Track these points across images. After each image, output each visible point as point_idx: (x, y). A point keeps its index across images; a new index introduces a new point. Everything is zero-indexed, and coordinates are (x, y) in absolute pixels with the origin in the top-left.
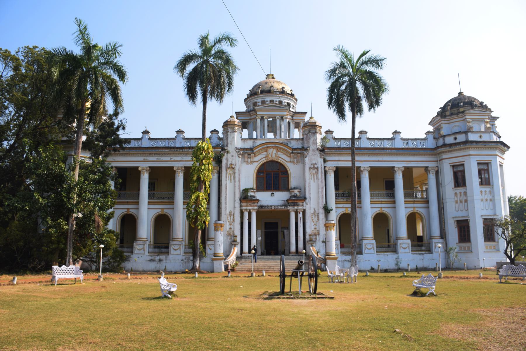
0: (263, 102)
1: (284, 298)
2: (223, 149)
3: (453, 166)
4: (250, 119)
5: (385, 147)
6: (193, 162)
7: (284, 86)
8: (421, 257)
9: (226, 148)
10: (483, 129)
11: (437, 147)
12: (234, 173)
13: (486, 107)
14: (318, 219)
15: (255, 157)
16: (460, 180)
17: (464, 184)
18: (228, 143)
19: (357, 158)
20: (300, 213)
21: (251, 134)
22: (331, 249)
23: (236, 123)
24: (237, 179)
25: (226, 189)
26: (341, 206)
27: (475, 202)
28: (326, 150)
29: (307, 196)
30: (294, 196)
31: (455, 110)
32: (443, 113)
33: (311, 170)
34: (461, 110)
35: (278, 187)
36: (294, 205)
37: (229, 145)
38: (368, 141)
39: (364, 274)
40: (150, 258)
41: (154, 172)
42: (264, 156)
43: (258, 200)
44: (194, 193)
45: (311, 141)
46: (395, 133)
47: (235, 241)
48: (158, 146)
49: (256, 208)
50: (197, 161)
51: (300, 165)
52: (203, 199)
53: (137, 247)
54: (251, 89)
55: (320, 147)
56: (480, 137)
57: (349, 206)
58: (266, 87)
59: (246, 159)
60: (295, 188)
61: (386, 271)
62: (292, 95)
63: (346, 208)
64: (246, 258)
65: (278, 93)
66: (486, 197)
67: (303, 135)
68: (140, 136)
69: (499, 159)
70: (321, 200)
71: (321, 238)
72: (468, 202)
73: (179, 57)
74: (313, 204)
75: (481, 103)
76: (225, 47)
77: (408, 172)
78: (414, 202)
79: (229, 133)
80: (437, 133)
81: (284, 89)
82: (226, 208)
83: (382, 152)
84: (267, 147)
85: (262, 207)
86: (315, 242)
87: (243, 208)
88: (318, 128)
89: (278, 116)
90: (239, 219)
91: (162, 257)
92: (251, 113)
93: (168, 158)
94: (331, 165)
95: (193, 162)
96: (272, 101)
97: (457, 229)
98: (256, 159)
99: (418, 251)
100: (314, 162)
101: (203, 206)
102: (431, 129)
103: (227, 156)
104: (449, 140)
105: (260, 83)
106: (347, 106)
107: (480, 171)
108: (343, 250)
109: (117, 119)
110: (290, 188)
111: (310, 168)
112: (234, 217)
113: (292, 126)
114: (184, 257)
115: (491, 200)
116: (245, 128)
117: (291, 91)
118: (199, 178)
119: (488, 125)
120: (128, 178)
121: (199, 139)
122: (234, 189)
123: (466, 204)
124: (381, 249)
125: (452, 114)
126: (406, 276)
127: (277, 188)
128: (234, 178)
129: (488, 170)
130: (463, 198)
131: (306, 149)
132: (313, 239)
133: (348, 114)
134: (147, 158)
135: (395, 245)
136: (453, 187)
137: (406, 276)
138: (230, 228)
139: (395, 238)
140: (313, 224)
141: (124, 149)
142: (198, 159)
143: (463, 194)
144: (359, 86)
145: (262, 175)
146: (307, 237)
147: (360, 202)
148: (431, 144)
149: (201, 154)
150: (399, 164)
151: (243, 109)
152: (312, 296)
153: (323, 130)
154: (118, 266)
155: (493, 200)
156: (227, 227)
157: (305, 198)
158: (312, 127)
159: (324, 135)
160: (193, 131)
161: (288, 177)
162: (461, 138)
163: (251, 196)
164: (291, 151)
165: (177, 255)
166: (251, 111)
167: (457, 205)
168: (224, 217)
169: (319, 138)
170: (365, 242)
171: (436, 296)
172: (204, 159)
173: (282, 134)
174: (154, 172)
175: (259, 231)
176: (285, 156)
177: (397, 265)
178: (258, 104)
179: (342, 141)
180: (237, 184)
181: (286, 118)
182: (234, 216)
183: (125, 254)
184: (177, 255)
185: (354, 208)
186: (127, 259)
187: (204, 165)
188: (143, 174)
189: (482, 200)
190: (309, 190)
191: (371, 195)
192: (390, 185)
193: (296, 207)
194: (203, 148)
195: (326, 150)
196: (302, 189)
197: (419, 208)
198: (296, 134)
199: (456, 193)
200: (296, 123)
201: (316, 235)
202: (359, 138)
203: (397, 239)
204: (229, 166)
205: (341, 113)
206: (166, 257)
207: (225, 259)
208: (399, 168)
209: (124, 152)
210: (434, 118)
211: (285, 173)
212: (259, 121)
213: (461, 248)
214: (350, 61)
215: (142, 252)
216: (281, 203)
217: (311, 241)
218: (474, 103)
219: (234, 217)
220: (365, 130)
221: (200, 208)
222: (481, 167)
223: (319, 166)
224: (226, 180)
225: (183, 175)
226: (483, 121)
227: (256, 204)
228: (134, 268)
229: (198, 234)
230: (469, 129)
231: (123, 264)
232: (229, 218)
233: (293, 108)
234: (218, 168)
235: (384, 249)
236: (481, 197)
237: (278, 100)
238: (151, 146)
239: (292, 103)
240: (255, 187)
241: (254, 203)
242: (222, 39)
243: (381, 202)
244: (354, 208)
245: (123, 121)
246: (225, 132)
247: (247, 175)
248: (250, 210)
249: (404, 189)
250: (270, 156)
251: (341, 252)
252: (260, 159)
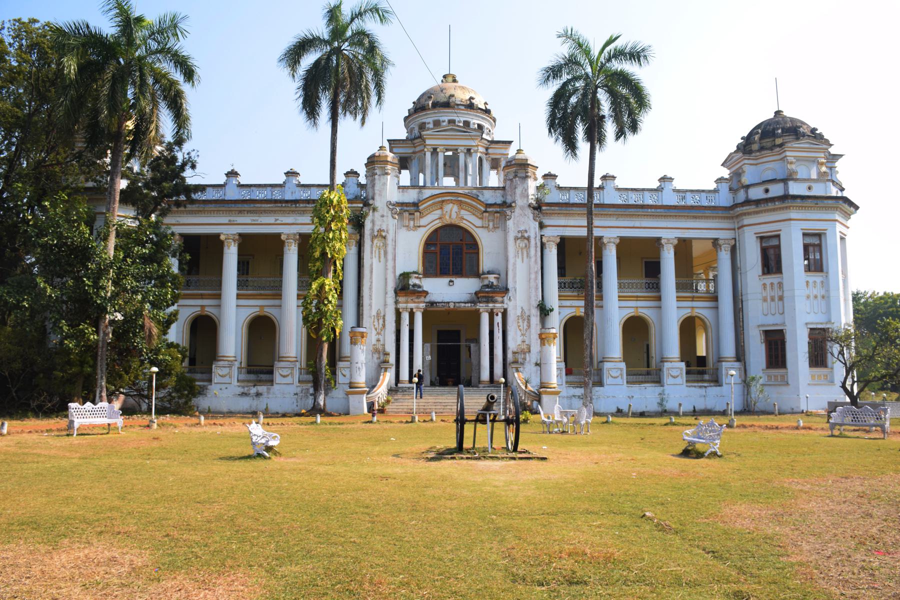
0: (437, 123)
1: (462, 458)
2: (366, 204)
3: (762, 238)
4: (414, 153)
5: (646, 203)
6: (313, 227)
7: (473, 96)
8: (702, 391)
9: (371, 202)
10: (814, 176)
11: (736, 206)
12: (385, 245)
13: (821, 136)
14: (529, 326)
15: (421, 217)
16: (772, 262)
17: (779, 270)
18: (374, 194)
19: (596, 222)
20: (497, 315)
21: (414, 179)
22: (550, 377)
23: (389, 159)
24: (390, 257)
25: (371, 272)
26: (568, 303)
27: (796, 298)
28: (544, 208)
29: (510, 286)
30: (487, 286)
31: (767, 142)
32: (747, 147)
33: (518, 241)
34: (779, 141)
35: (461, 270)
36: (488, 302)
37: (377, 197)
38: (617, 193)
39: (604, 419)
40: (242, 390)
41: (247, 243)
42: (437, 217)
43: (426, 293)
44: (316, 279)
45: (518, 191)
46: (664, 179)
47: (386, 362)
48: (253, 198)
49: (422, 305)
50: (321, 225)
51: (499, 233)
52: (331, 290)
53: (218, 371)
54: (415, 100)
55: (534, 203)
56: (809, 188)
57: (582, 303)
58: (442, 98)
59: (406, 222)
60: (489, 273)
61: (642, 415)
62: (487, 111)
63: (576, 307)
64: (404, 390)
65: (463, 108)
66: (815, 292)
67: (505, 180)
68: (222, 180)
69: (839, 228)
70: (533, 293)
71: (533, 357)
72: (785, 299)
73: (289, 40)
74: (520, 300)
75: (814, 130)
76: (370, 25)
77: (683, 248)
78: (693, 299)
79: (376, 177)
80: (734, 179)
81: (473, 101)
82: (371, 305)
83: (640, 211)
84: (443, 201)
85: (432, 303)
86: (522, 364)
87: (401, 306)
88: (530, 169)
89: (462, 148)
90: (394, 324)
91: (262, 389)
92: (416, 141)
93: (270, 219)
94: (553, 234)
95: (313, 227)
96: (451, 122)
97: (764, 345)
98: (423, 221)
99: (698, 381)
100: (522, 228)
101: (330, 302)
102: (725, 173)
103: (373, 215)
104: (756, 193)
105: (431, 89)
106: (580, 131)
107: (806, 247)
108: (571, 378)
109: (181, 150)
110: (481, 272)
111: (516, 239)
112: (384, 322)
113: (486, 165)
114: (299, 389)
115: (823, 297)
116: (406, 168)
117: (486, 103)
118: (324, 254)
119: (824, 169)
120: (202, 253)
121: (326, 186)
122: (386, 274)
123: (780, 303)
124: (634, 378)
125: (762, 149)
126: (674, 424)
127: (459, 272)
128: (386, 253)
129: (819, 246)
130: (776, 293)
131: (510, 206)
132: (520, 360)
133: (583, 147)
134: (235, 219)
135: (659, 371)
136: (760, 273)
137: (674, 424)
138: (378, 340)
139: (658, 360)
140: (519, 333)
141: (193, 202)
142: (322, 220)
143: (776, 286)
144: (603, 96)
145: (433, 248)
146: (510, 356)
147: (601, 298)
148: (724, 199)
149: (328, 212)
150: (668, 232)
151: (402, 134)
152: (510, 455)
153: (540, 173)
154: (186, 403)
155: (826, 297)
156: (372, 337)
157: (506, 290)
158: (519, 168)
159: (540, 181)
160: (314, 172)
161: (478, 253)
162: (776, 190)
163: (414, 285)
164: (483, 209)
165: (287, 385)
166: (416, 138)
167: (765, 304)
168: (366, 320)
169: (532, 186)
170: (607, 365)
171: (720, 456)
172: (332, 221)
173: (469, 178)
174: (247, 243)
175: (428, 345)
176: (474, 217)
177: (661, 404)
178: (427, 126)
179: (572, 192)
180: (390, 264)
181: (476, 152)
182: (384, 319)
183: (197, 383)
184: (287, 385)
185: (589, 307)
186: (202, 392)
187: (333, 231)
188: (229, 247)
189: (808, 297)
190: (515, 276)
191: (620, 286)
192: (653, 270)
193: (491, 305)
194: (331, 201)
195: (544, 208)
196: (502, 274)
197: (701, 309)
198: (494, 179)
199: (764, 285)
200: (493, 159)
201: (525, 353)
202: (601, 188)
203: (662, 362)
204: (376, 234)
205: (571, 145)
206: (269, 389)
207: (368, 393)
208: (668, 240)
209: (194, 207)
210: (731, 154)
211: (474, 246)
212: (428, 155)
213: (769, 377)
214: (587, 52)
215: (226, 380)
216: (465, 297)
217: (516, 362)
218: (801, 130)
219: (384, 322)
220: (611, 174)
221: (326, 305)
222: (809, 240)
223: (532, 235)
224: (372, 258)
225: (296, 248)
226: (814, 161)
227: (422, 299)
228: (213, 408)
229: (322, 350)
230: (791, 175)
231: (194, 401)
232: (376, 323)
233: (488, 134)
234: (358, 237)
235: (641, 378)
236: (807, 292)
237: (462, 119)
238: (241, 198)
239: (486, 125)
240: (421, 270)
241: (418, 297)
242: (365, 12)
243: (637, 298)
244: (589, 307)
245: (193, 154)
246: (371, 174)
247: (407, 248)
248: (412, 309)
249: (677, 276)
250: (447, 217)
251: (567, 382)
252: (431, 221)
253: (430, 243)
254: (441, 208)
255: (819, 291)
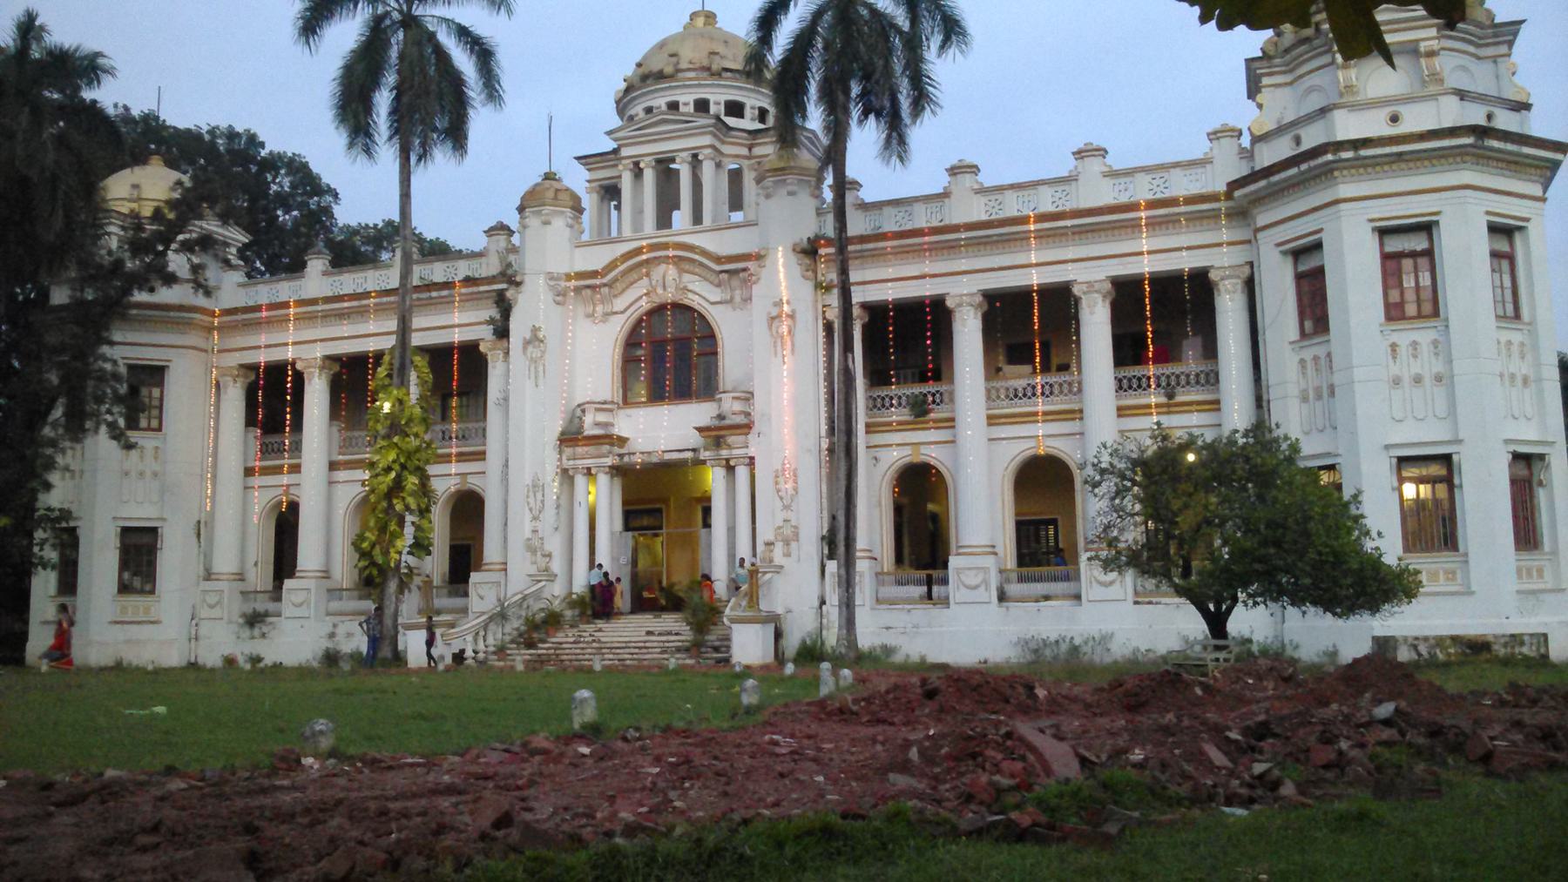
27: (1357, 387)
89: (684, 154)
98: (619, 304)
107: (1391, 262)
115: (1439, 379)
138: (535, 531)
146: (760, 548)
176: (705, 283)
222: (1396, 244)
232: (531, 500)
252: (634, 300)
253: (632, 342)
254: (648, 275)
255: (1428, 365)
